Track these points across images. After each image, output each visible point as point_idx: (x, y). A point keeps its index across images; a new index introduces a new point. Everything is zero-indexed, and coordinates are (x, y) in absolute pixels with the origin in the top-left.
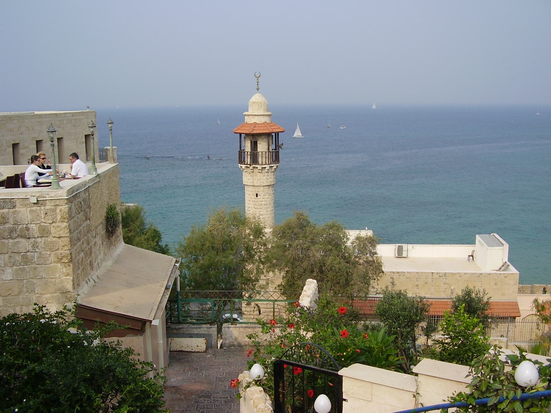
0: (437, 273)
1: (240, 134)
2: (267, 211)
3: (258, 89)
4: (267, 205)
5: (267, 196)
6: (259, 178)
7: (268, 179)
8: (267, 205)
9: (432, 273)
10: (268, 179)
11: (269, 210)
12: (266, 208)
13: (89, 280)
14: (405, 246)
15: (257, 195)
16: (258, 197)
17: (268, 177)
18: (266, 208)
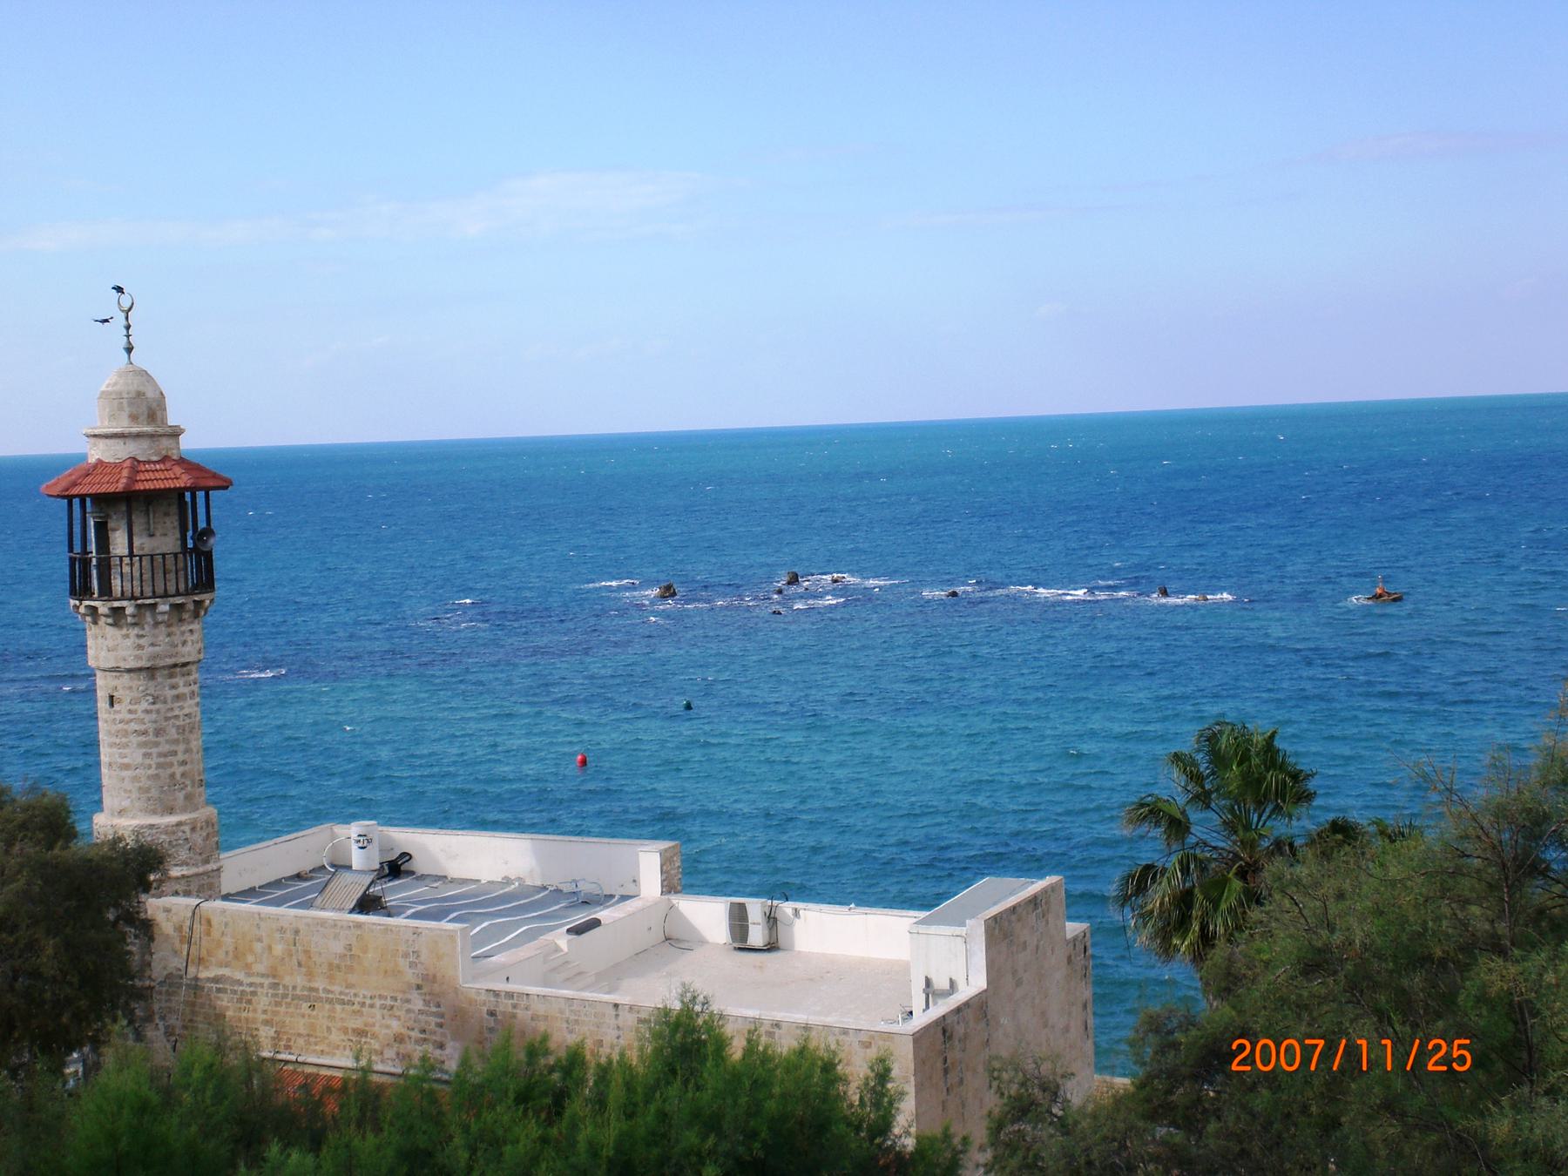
0: (631, 1008)
1: (70, 498)
2: (146, 755)
3: (129, 350)
4: (145, 733)
5: (144, 705)
6: (110, 643)
7: (140, 647)
8: (145, 733)
9: (616, 1006)
10: (140, 647)
11: (154, 751)
12: (140, 745)
13: (441, 1025)
14: (787, 908)
15: (112, 705)
16: (117, 707)
17: (142, 641)
18: (140, 745)
